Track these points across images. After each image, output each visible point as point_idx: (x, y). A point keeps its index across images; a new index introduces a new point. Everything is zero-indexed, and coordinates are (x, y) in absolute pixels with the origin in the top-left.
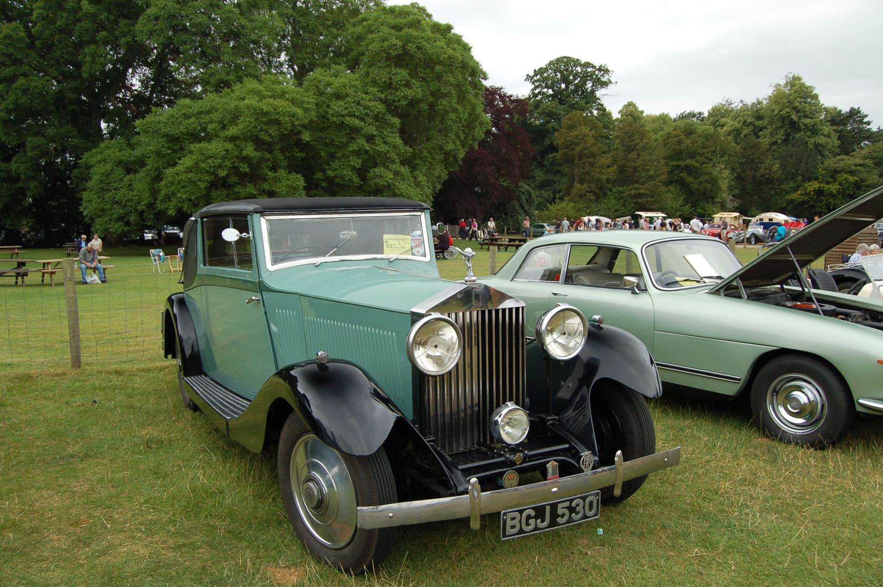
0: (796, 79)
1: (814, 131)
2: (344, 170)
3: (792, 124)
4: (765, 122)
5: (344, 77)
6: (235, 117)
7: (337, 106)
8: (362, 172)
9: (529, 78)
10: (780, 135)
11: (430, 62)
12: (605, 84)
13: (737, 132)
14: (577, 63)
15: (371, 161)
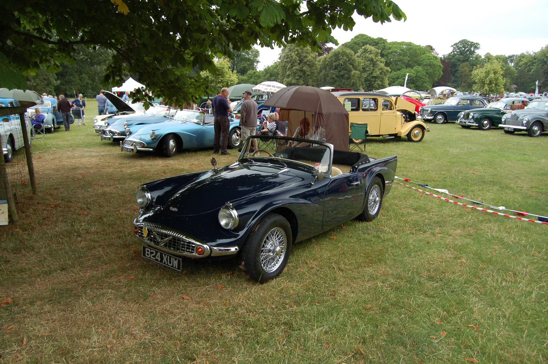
2: (419, 84)
4: (537, 60)
5: (420, 68)
7: (419, 74)
8: (422, 84)
11: (434, 65)
12: (478, 48)
13: (527, 63)
15: (423, 82)
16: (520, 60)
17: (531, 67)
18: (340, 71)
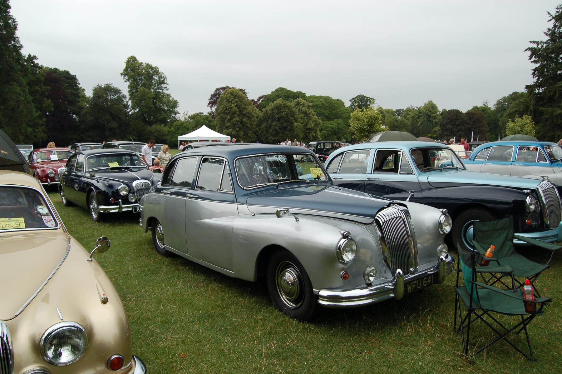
0: (431, 101)
1: (435, 118)
3: (429, 116)
4: (422, 114)
5: (340, 121)
6: (328, 128)
7: (340, 126)
9: (350, 100)
10: (425, 119)
12: (373, 103)
13: (414, 117)
14: (365, 97)
16: (407, 114)
17: (418, 120)
18: (282, 123)
